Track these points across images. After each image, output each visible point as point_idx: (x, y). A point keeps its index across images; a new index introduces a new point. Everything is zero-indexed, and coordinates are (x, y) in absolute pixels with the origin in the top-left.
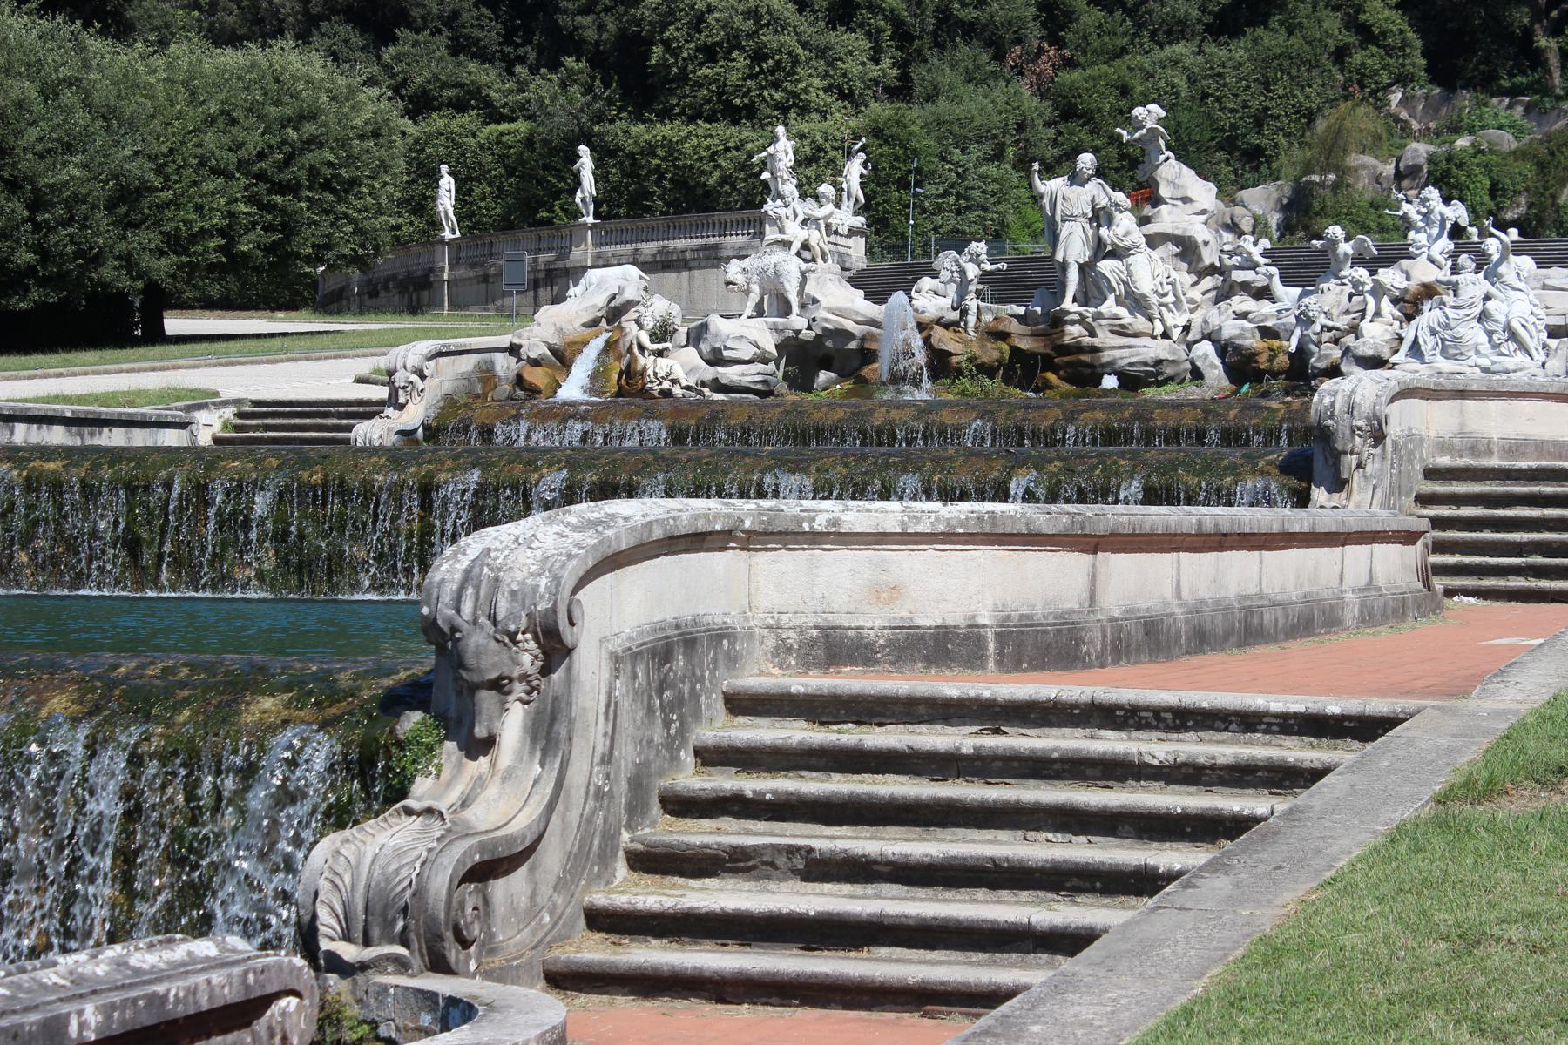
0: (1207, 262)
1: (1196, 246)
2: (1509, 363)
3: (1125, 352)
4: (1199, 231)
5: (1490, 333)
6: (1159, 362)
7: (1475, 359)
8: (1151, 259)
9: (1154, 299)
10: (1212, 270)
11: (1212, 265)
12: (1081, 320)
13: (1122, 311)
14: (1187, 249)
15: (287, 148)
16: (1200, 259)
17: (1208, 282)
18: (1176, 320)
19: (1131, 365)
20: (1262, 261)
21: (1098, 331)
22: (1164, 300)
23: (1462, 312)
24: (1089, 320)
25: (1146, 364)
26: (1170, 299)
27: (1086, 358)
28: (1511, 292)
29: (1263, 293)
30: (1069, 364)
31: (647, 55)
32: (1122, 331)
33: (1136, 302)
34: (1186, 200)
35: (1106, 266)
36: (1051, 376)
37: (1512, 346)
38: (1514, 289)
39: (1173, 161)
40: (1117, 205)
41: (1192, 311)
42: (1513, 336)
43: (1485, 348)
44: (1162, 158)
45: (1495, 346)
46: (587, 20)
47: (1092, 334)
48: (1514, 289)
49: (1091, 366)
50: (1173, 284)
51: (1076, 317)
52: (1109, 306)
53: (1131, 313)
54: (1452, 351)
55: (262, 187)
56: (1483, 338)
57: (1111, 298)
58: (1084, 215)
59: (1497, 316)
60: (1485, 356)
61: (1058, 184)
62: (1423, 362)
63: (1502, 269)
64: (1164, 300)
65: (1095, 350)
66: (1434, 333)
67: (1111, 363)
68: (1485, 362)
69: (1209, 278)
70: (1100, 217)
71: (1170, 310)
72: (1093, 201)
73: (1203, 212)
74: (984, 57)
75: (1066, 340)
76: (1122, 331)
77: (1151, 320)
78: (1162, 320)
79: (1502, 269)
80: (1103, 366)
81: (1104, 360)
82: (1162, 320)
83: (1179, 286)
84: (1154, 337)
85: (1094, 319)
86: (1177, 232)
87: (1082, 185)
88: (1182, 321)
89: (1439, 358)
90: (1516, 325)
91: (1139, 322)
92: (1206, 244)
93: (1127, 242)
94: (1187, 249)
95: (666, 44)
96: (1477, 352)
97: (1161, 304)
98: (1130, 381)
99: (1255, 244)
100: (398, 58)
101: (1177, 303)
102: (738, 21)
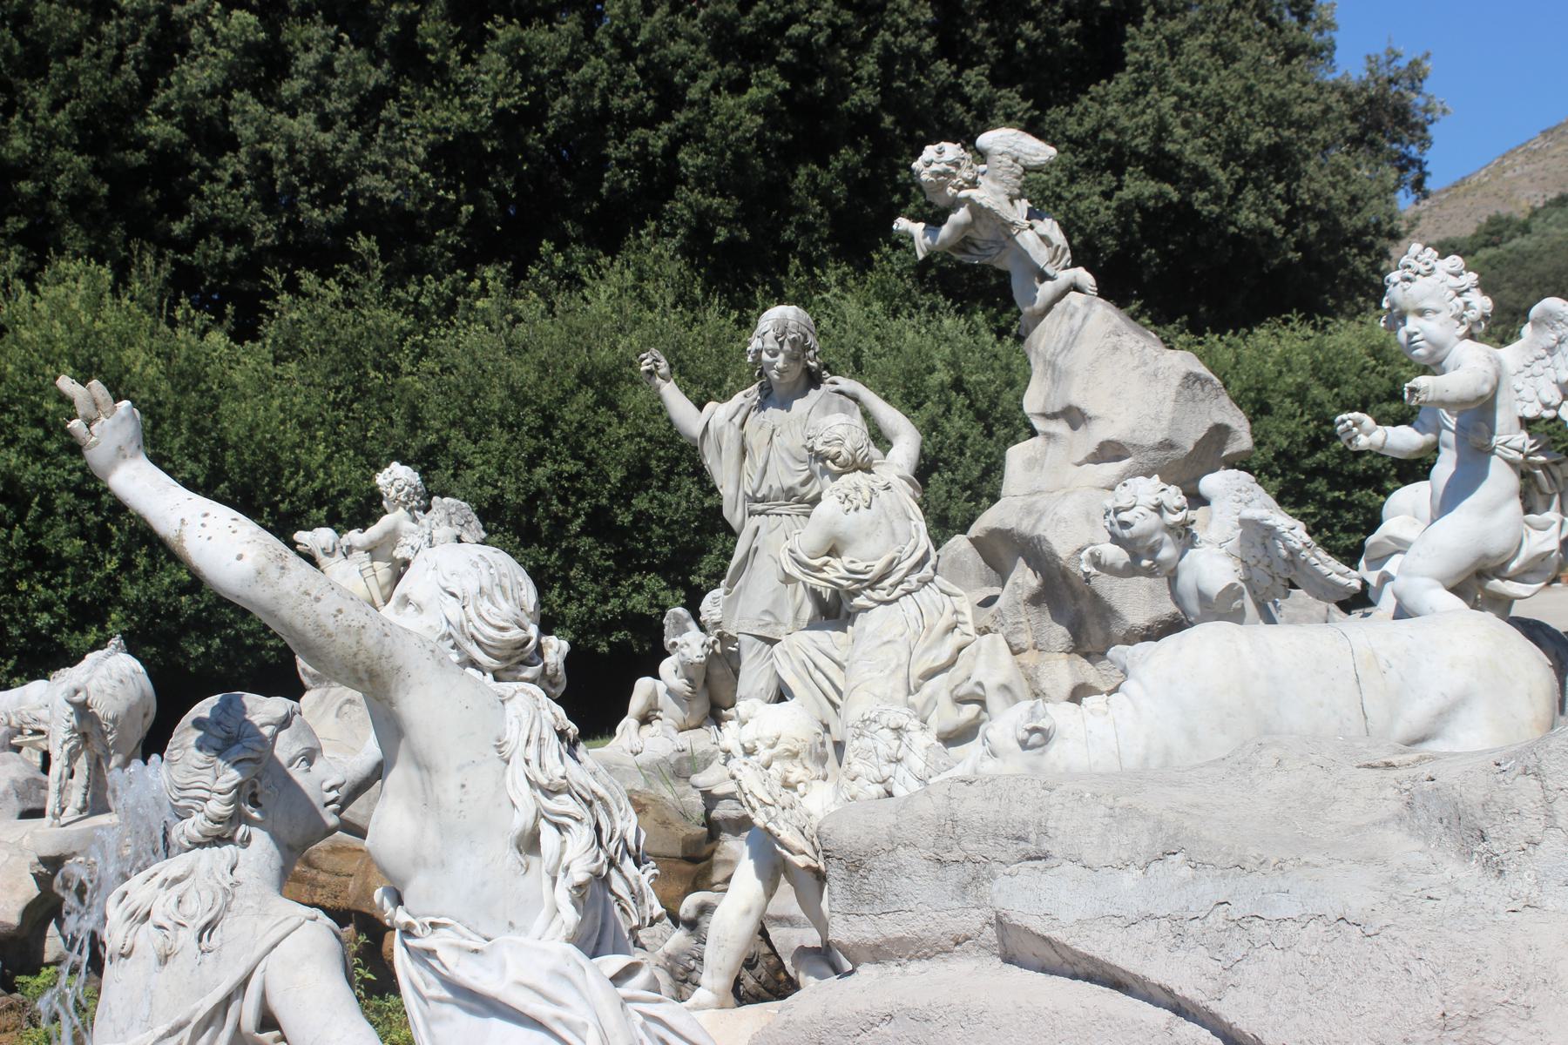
34: (1074, 416)
44: (1045, 290)
55: (1320, 485)
87: (785, 405)
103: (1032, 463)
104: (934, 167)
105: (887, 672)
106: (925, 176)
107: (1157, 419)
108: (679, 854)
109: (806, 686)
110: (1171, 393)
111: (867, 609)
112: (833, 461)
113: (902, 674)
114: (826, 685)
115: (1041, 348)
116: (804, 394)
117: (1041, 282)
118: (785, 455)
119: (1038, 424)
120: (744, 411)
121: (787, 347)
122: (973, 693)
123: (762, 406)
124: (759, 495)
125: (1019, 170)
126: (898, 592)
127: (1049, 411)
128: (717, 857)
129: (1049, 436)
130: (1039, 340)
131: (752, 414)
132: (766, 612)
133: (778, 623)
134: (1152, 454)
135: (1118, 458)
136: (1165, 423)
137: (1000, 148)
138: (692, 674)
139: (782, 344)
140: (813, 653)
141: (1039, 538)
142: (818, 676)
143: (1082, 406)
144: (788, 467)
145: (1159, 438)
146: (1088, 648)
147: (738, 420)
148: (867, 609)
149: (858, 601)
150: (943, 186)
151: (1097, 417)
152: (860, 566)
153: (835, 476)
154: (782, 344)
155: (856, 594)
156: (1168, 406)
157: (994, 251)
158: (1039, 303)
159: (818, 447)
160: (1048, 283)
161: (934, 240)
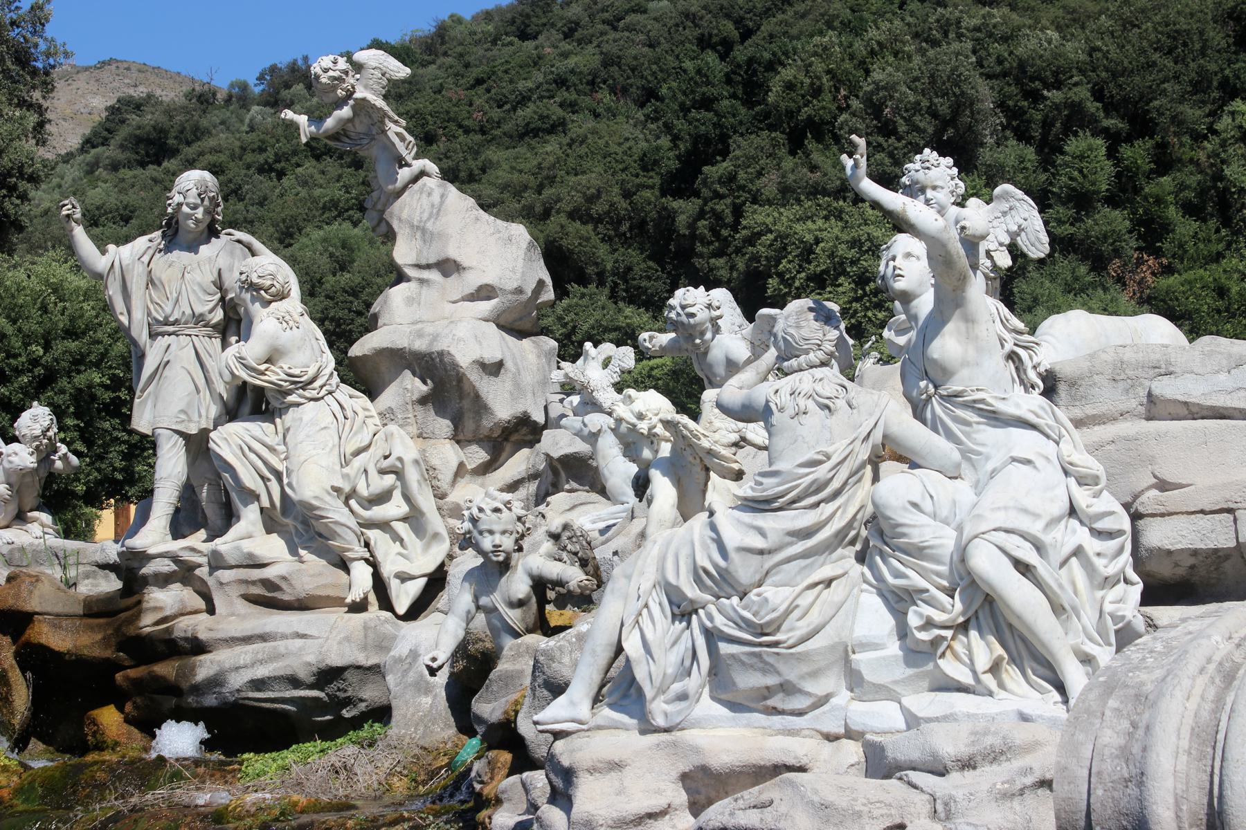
1: (460, 378)
2: (953, 722)
3: (243, 654)
4: (469, 338)
5: (899, 601)
6: (328, 675)
7: (848, 708)
9: (336, 512)
10: (524, 431)
12: (184, 573)
13: (273, 547)
14: (448, 390)
15: (39, 371)
16: (480, 406)
17: (519, 463)
18: (407, 561)
19: (258, 684)
21: (218, 602)
22: (378, 512)
23: (777, 523)
24: (202, 572)
25: (294, 682)
26: (396, 508)
27: (166, 669)
28: (988, 435)
30: (139, 686)
31: (765, 289)
32: (269, 597)
33: (298, 523)
34: (448, 267)
35: (234, 442)
36: (109, 718)
37: (983, 649)
38: (995, 418)
39: (433, 183)
40: (252, 287)
42: (985, 611)
43: (882, 657)
44: (404, 174)
45: (919, 654)
46: (720, 262)
47: (211, 610)
48: (995, 418)
49: (173, 689)
50: (399, 473)
51: (166, 566)
52: (248, 535)
53: (293, 551)
54: (748, 680)
56: (873, 618)
57: (250, 516)
58: (198, 319)
59: (922, 529)
60: (883, 692)
61: (133, 253)
62: (647, 728)
63: (947, 346)
64: (378, 512)
65: (199, 647)
66: (683, 611)
67: (216, 682)
68: (880, 717)
69: (525, 452)
71: (397, 538)
72: (219, 285)
73: (484, 292)
74: (1083, 270)
75: (147, 623)
76: (269, 597)
77: (343, 565)
78: (373, 564)
79: (947, 346)
80: (197, 689)
81: (202, 674)
82: (373, 564)
83: (412, 475)
84: (359, 607)
85: (213, 568)
86: (420, 345)
87: (193, 248)
88: (426, 562)
89: (707, 707)
90: (990, 565)
91: (309, 573)
92: (494, 369)
93: (274, 376)
94: (448, 390)
95: (781, 275)
96: (854, 680)
98: (245, 727)
100: (567, 310)
101: (414, 518)
102: (842, 250)
103: (410, 301)
104: (331, 73)
105: (328, 450)
106: (324, 79)
107: (513, 271)
108: (81, 612)
109: (244, 465)
110: (521, 253)
111: (298, 405)
113: (336, 452)
114: (260, 464)
115: (405, 215)
116: (208, 241)
117: (401, 166)
118: (196, 288)
119: (410, 272)
120: (151, 252)
121: (206, 202)
122: (394, 466)
123: (168, 249)
124: (171, 319)
125: (385, 82)
126: (323, 392)
127: (424, 262)
128: (145, 605)
129: (422, 281)
130: (401, 209)
132: (183, 411)
133: (190, 420)
134: (510, 297)
135: (489, 298)
136: (519, 275)
137: (374, 64)
138: (13, 479)
139: (203, 200)
141: (441, 354)
143: (458, 259)
144: (199, 298)
145: (515, 285)
146: (461, 437)
147: (146, 259)
148: (298, 405)
149: (291, 398)
150: (334, 88)
151: (470, 268)
152: (296, 371)
153: (267, 304)
154: (203, 200)
155: (289, 393)
156: (520, 263)
157: (365, 142)
158: (399, 184)
159: (255, 280)
160: (406, 169)
161: (318, 129)
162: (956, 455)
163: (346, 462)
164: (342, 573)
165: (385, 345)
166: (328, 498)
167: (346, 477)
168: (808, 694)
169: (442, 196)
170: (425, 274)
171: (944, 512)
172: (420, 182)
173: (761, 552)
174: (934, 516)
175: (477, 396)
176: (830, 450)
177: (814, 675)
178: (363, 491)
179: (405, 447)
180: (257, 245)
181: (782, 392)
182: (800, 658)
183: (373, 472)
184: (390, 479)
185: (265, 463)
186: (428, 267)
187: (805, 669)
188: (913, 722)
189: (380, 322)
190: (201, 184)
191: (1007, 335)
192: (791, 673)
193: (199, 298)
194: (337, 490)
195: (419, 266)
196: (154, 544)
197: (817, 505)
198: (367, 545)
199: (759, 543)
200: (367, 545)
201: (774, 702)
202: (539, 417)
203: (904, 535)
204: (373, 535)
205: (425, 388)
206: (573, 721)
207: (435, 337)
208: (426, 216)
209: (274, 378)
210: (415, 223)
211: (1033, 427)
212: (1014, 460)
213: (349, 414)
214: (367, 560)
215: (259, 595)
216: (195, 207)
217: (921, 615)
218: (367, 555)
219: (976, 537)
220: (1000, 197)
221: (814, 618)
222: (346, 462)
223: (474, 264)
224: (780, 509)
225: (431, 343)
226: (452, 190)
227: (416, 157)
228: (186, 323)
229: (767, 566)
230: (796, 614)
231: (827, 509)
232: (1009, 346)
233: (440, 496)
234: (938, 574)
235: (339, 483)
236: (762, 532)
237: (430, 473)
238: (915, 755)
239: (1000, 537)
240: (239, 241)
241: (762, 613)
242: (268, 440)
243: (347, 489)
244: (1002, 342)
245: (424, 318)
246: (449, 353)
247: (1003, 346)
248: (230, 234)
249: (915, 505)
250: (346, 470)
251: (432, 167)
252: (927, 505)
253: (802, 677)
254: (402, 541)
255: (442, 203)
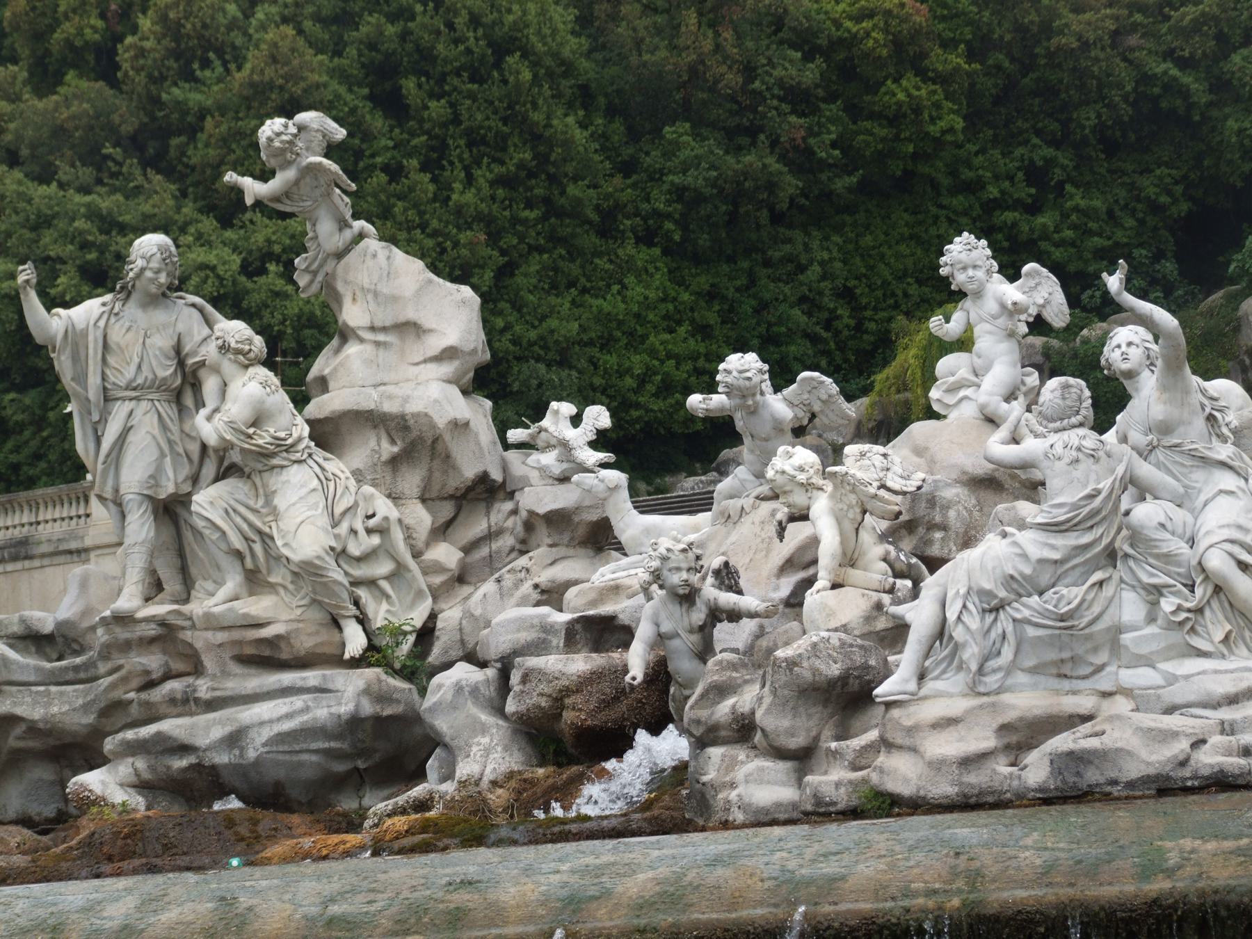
0: (470, 471)
8: (324, 479)
11: (484, 478)
20: (592, 457)
29: (600, 538)
39: (373, 244)
41: (436, 594)
48: (1206, 462)
70: (185, 384)
73: (448, 354)
82: (362, 621)
83: (398, 535)
97: (356, 583)
99: (576, 420)
104: (284, 138)
111: (282, 467)
112: (244, 355)
114: (245, 527)
120: (105, 316)
124: (134, 385)
125: (325, 145)
127: (378, 324)
129: (378, 344)
131: (113, 320)
134: (467, 358)
136: (474, 337)
137: (315, 126)
140: (232, 502)
142: (238, 520)
145: (472, 347)
147: (102, 323)
148: (282, 467)
149: (276, 461)
151: (430, 331)
152: (282, 434)
162: (1182, 490)
163: (335, 525)
164: (336, 631)
165: (349, 407)
166: (327, 558)
167: (337, 537)
168: (1092, 664)
169: (389, 258)
170: (381, 337)
171: (1180, 531)
172: (362, 244)
173: (1056, 562)
174: (1173, 533)
175: (448, 457)
176: (1100, 486)
177: (1095, 650)
178: (355, 550)
179: (384, 508)
180: (209, 308)
181: (1056, 446)
182: (1088, 638)
183: (362, 532)
184: (376, 540)
185: (251, 525)
186: (384, 329)
187: (1089, 645)
188: (1172, 679)
189: (332, 385)
190: (162, 249)
191: (1206, 402)
192: (1080, 650)
193: (161, 364)
194: (332, 549)
195: (372, 329)
196: (138, 609)
197: (1092, 527)
198: (356, 603)
199: (1056, 556)
200: (356, 603)
201: (1066, 669)
202: (496, 475)
203: (1156, 547)
204: (362, 593)
205: (396, 449)
206: (905, 693)
207: (406, 400)
208: (375, 278)
209: (261, 442)
210: (366, 286)
211: (1231, 468)
212: (1221, 491)
213: (331, 477)
214: (357, 618)
215: (252, 655)
216: (158, 272)
217: (1172, 603)
218: (358, 613)
219: (1211, 546)
220: (1028, 274)
221: (1096, 609)
222: (335, 525)
223: (434, 326)
224: (1066, 531)
225: (402, 406)
226: (398, 254)
227: (356, 216)
228: (149, 388)
229: (1059, 572)
230: (1085, 605)
231: (1097, 532)
232: (1208, 410)
233: (416, 555)
234: (1179, 574)
235: (334, 544)
236: (1053, 547)
237: (408, 530)
238: (1192, 698)
239: (1228, 546)
240: (194, 305)
241: (1061, 606)
242: (251, 503)
243: (339, 548)
244: (1203, 407)
245: (386, 380)
246: (426, 415)
247: (1203, 409)
248: (181, 298)
249: (1163, 525)
250: (336, 531)
251: (369, 227)
252: (1169, 525)
253: (1087, 652)
254: (388, 597)
255: (390, 265)
